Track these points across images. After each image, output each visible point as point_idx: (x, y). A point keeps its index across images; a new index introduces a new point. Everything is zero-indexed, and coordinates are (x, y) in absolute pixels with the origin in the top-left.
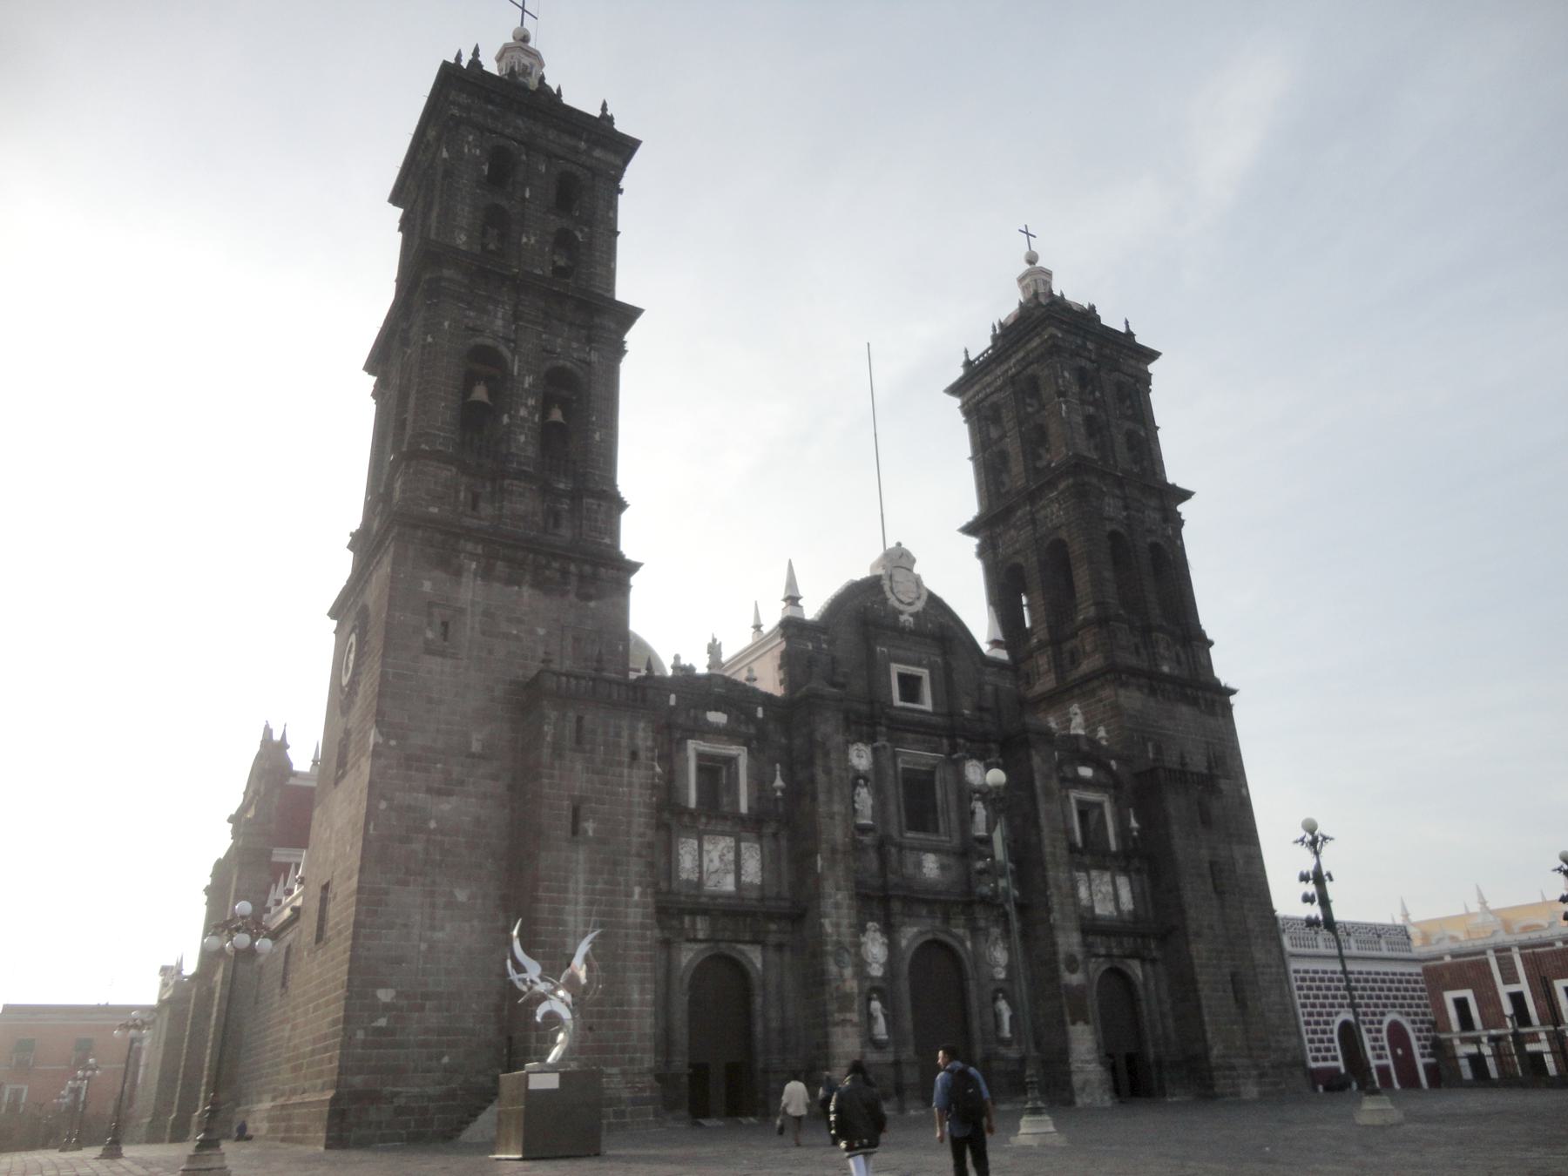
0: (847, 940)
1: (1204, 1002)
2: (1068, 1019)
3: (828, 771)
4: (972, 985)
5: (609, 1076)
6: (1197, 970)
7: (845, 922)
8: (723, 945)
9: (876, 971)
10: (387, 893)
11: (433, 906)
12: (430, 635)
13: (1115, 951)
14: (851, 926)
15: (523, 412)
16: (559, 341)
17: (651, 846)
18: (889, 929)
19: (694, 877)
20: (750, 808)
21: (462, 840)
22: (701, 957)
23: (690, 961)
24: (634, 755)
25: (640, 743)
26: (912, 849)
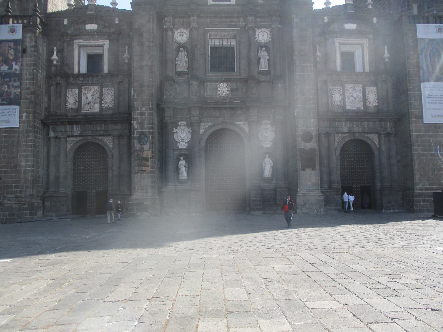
0: (146, 131)
5: (9, 198)
7: (146, 122)
8: (89, 138)
9: (183, 146)
13: (356, 130)
14: (149, 124)
18: (190, 125)
19: (76, 107)
20: (108, 71)
22: (78, 145)
26: (211, 81)
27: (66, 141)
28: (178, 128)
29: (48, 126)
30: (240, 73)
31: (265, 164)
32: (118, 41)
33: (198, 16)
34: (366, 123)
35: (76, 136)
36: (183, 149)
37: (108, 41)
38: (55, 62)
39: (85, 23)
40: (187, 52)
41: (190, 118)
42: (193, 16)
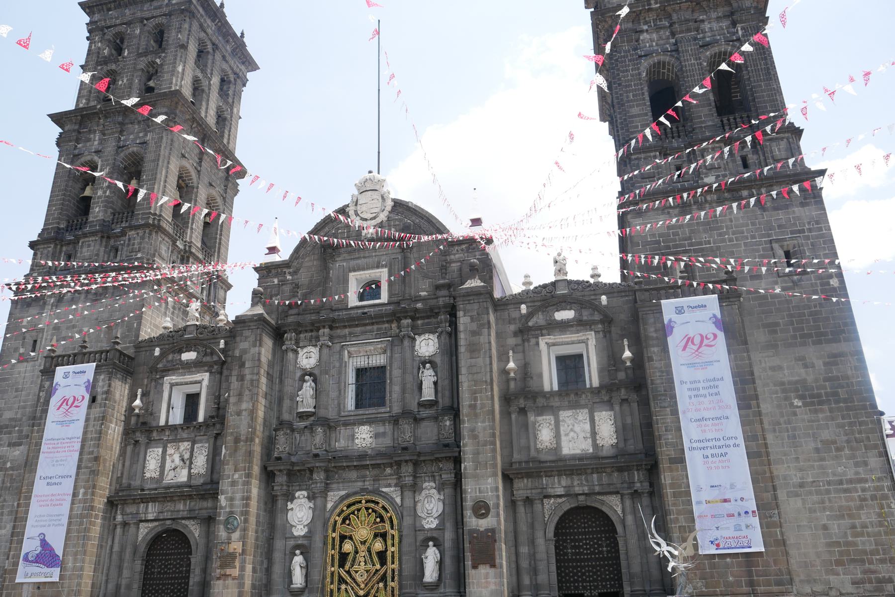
0: (238, 510)
2: (469, 563)
3: (241, 378)
7: (238, 496)
8: (168, 522)
9: (300, 531)
12: (22, 350)
13: (577, 490)
15: (100, 193)
16: (132, 137)
19: (156, 475)
23: (146, 535)
26: (346, 424)
27: (138, 528)
28: (295, 501)
29: (117, 505)
30: (390, 407)
31: (426, 558)
32: (221, 373)
33: (331, 328)
34: (595, 476)
35: (152, 521)
36: (299, 537)
37: (207, 374)
38: (137, 411)
39: (181, 351)
40: (315, 381)
42: (324, 327)
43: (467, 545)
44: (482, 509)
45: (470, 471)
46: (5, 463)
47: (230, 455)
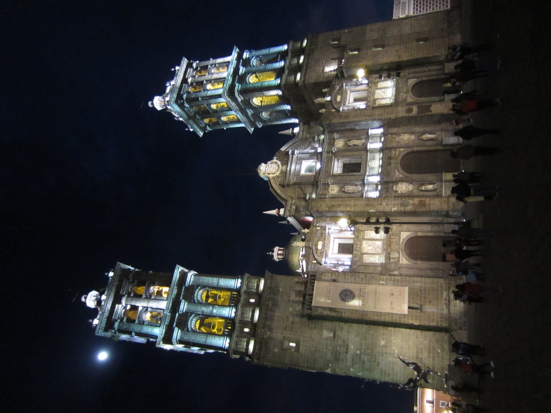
1: (425, 56)
2: (430, 113)
4: (415, 149)
6: (413, 58)
7: (393, 202)
10: (382, 370)
11: (386, 353)
12: (293, 350)
17: (365, 276)
18: (396, 182)
21: (363, 342)
24: (334, 281)
25: (330, 278)
39: (317, 249)
41: (392, 182)
43: (423, 114)
44: (410, 110)
45: (395, 115)
46: (357, 355)
47: (374, 208)
